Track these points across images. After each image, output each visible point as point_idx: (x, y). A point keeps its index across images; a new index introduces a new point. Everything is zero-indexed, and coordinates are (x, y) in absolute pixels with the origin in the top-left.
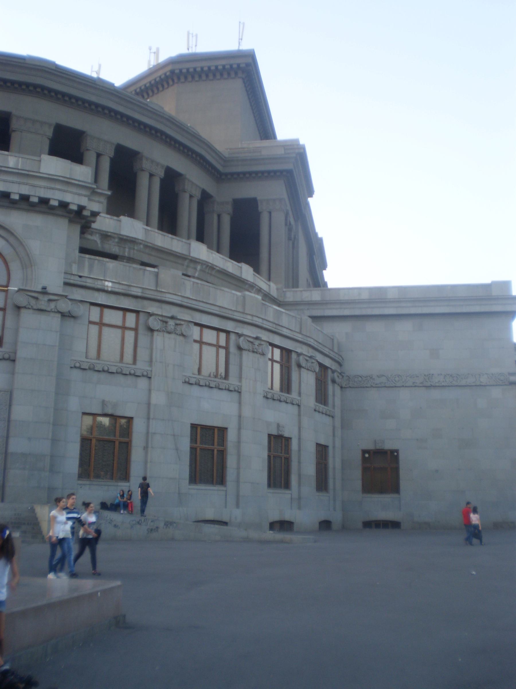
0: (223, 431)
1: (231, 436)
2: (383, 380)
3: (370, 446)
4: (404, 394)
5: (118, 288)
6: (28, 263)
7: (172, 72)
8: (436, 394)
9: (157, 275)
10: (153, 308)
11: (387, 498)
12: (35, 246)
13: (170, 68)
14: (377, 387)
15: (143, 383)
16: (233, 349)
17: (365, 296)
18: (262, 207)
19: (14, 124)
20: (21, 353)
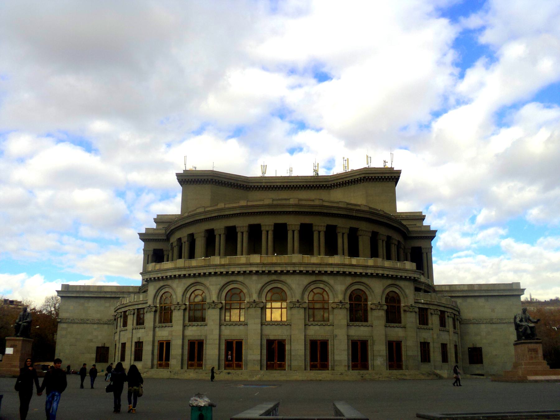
0: (446, 344)
1: (448, 345)
2: (475, 321)
3: (471, 346)
4: (483, 326)
5: (425, 302)
6: (406, 296)
7: (364, 177)
8: (494, 326)
9: (431, 296)
10: (431, 307)
11: (479, 366)
12: (407, 291)
13: (363, 175)
14: (474, 323)
15: (431, 331)
16: (446, 317)
17: (466, 288)
18: (423, 251)
19: (359, 233)
20: (408, 325)
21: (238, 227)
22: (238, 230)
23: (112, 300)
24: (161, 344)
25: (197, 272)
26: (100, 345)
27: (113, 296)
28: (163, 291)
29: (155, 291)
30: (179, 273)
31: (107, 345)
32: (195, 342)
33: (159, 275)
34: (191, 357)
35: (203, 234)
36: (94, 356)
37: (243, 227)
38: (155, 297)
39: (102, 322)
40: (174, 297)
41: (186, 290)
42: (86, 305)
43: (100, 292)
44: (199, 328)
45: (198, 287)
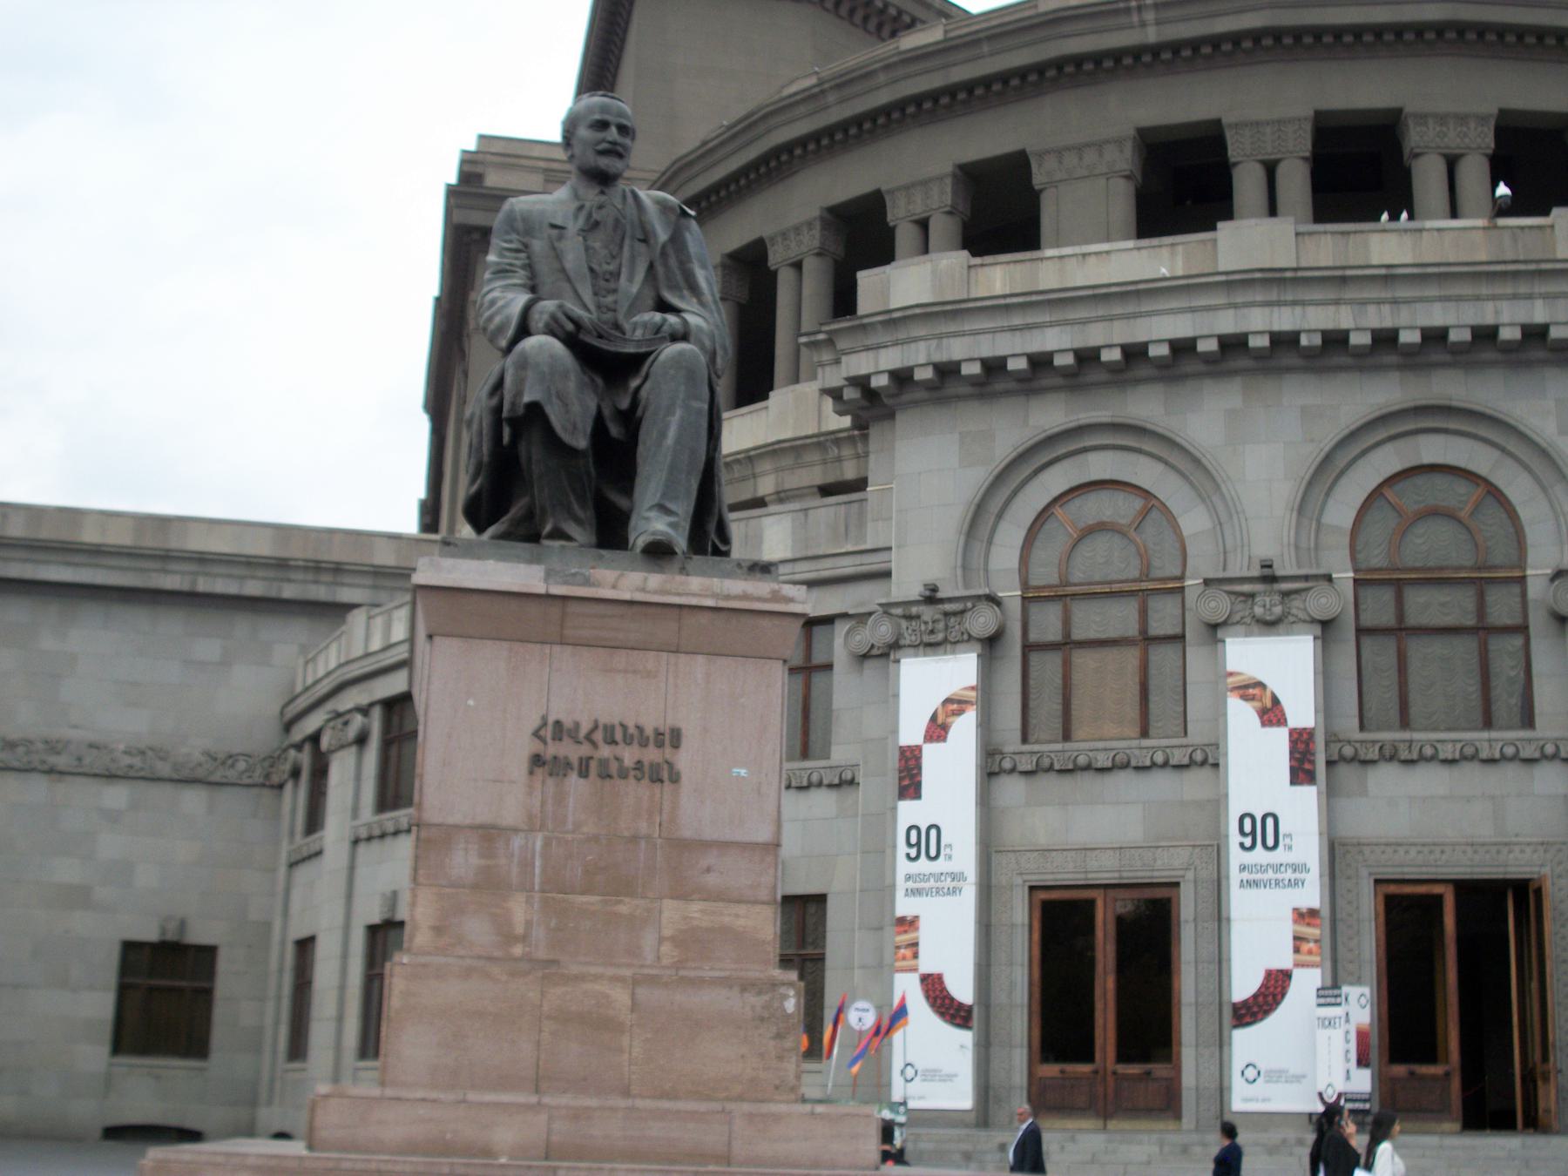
21: (1422, 118)
22: (1414, 137)
23: (242, 626)
24: (1062, 921)
25: (1457, 316)
26: (150, 934)
27: (253, 588)
28: (1056, 480)
29: (977, 477)
30: (1284, 320)
31: (198, 935)
32: (1438, 900)
33: (1058, 340)
34: (1061, 1029)
35: (1125, 159)
36: (100, 1005)
37: (1462, 119)
38: (979, 521)
39: (164, 769)
40: (1194, 521)
41: (1326, 472)
42: (48, 643)
43: (166, 557)
44: (1472, 778)
45: (1433, 449)
